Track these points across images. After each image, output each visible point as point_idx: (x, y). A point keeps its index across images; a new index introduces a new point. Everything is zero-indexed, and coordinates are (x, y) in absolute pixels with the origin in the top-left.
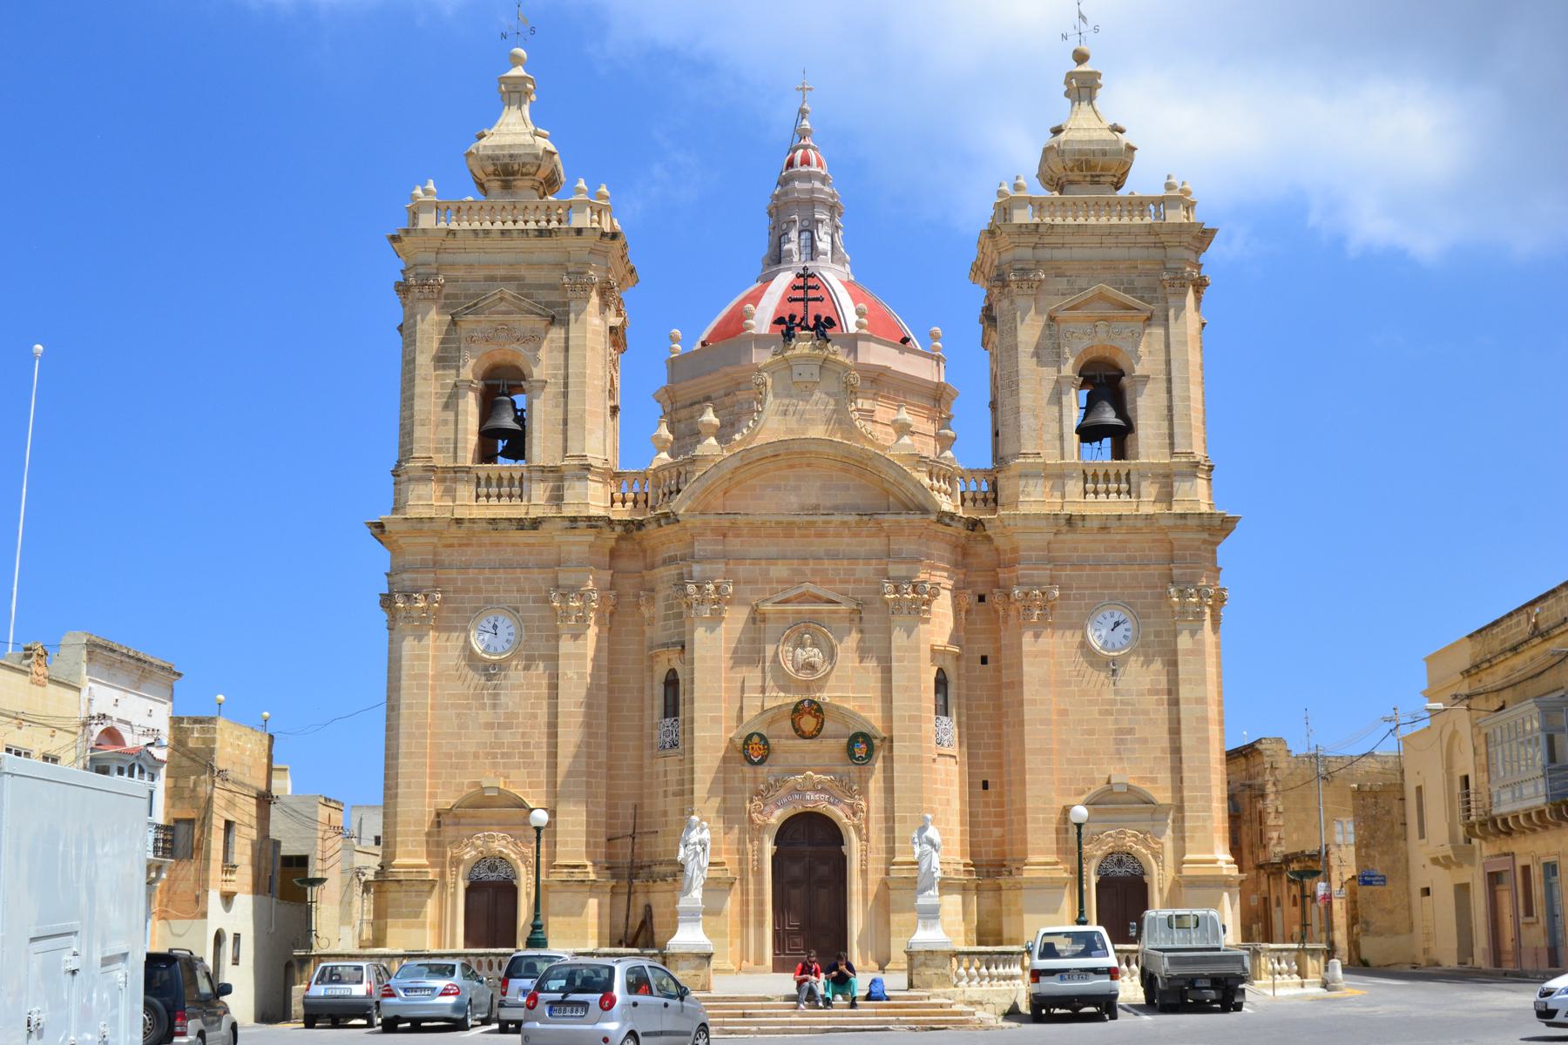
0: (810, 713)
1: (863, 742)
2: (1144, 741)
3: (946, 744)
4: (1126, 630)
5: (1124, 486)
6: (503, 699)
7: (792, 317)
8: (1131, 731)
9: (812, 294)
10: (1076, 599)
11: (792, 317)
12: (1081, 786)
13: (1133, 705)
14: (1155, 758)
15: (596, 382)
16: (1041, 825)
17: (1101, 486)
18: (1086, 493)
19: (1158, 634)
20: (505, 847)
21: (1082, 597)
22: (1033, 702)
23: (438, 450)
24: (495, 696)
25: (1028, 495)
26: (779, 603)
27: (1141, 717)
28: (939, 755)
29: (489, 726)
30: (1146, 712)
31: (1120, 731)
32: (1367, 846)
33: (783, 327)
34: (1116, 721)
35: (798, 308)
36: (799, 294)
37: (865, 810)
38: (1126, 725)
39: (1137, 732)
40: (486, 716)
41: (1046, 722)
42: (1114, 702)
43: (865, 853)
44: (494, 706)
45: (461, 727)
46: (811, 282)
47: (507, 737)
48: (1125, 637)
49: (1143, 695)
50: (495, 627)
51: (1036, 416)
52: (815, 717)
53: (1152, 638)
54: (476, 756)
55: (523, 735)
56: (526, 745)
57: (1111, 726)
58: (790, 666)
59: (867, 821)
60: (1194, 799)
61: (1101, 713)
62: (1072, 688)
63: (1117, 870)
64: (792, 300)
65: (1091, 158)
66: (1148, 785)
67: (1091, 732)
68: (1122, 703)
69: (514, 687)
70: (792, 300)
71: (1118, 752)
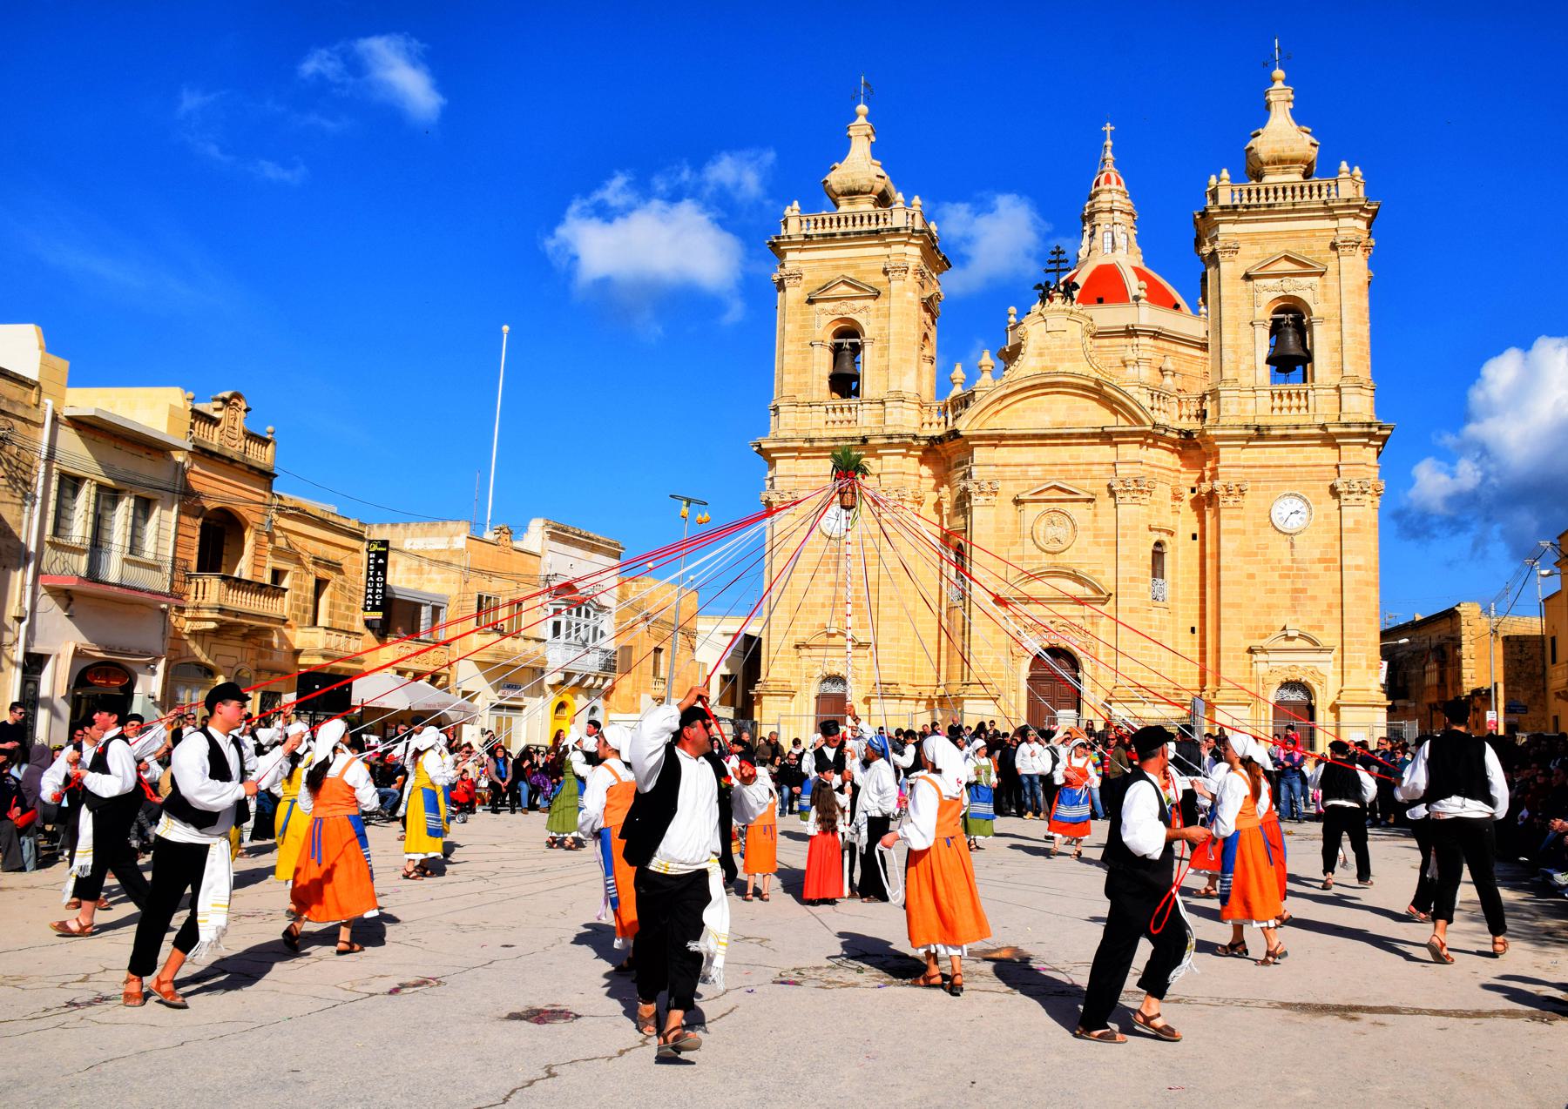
2: (1314, 598)
3: (1161, 599)
5: (1303, 403)
7: (1048, 284)
8: (1304, 591)
10: (1263, 490)
11: (1048, 284)
12: (1264, 631)
13: (1306, 570)
14: (1322, 611)
17: (1286, 402)
19: (1327, 516)
21: (1268, 488)
22: (1228, 568)
23: (800, 391)
25: (1227, 411)
27: (1313, 580)
29: (831, 584)
30: (1316, 577)
31: (1296, 591)
32: (1513, 684)
33: (1041, 291)
34: (1293, 582)
35: (1051, 277)
36: (1053, 266)
38: (1299, 586)
41: (1238, 583)
42: (1291, 568)
46: (1062, 257)
49: (1314, 563)
51: (1235, 352)
53: (1323, 519)
54: (823, 606)
55: (856, 591)
58: (1042, 539)
60: (1351, 643)
61: (1281, 576)
64: (1047, 271)
65: (1282, 154)
66: (1317, 632)
67: (1273, 591)
68: (1298, 569)
70: (1047, 271)
71: (1293, 606)
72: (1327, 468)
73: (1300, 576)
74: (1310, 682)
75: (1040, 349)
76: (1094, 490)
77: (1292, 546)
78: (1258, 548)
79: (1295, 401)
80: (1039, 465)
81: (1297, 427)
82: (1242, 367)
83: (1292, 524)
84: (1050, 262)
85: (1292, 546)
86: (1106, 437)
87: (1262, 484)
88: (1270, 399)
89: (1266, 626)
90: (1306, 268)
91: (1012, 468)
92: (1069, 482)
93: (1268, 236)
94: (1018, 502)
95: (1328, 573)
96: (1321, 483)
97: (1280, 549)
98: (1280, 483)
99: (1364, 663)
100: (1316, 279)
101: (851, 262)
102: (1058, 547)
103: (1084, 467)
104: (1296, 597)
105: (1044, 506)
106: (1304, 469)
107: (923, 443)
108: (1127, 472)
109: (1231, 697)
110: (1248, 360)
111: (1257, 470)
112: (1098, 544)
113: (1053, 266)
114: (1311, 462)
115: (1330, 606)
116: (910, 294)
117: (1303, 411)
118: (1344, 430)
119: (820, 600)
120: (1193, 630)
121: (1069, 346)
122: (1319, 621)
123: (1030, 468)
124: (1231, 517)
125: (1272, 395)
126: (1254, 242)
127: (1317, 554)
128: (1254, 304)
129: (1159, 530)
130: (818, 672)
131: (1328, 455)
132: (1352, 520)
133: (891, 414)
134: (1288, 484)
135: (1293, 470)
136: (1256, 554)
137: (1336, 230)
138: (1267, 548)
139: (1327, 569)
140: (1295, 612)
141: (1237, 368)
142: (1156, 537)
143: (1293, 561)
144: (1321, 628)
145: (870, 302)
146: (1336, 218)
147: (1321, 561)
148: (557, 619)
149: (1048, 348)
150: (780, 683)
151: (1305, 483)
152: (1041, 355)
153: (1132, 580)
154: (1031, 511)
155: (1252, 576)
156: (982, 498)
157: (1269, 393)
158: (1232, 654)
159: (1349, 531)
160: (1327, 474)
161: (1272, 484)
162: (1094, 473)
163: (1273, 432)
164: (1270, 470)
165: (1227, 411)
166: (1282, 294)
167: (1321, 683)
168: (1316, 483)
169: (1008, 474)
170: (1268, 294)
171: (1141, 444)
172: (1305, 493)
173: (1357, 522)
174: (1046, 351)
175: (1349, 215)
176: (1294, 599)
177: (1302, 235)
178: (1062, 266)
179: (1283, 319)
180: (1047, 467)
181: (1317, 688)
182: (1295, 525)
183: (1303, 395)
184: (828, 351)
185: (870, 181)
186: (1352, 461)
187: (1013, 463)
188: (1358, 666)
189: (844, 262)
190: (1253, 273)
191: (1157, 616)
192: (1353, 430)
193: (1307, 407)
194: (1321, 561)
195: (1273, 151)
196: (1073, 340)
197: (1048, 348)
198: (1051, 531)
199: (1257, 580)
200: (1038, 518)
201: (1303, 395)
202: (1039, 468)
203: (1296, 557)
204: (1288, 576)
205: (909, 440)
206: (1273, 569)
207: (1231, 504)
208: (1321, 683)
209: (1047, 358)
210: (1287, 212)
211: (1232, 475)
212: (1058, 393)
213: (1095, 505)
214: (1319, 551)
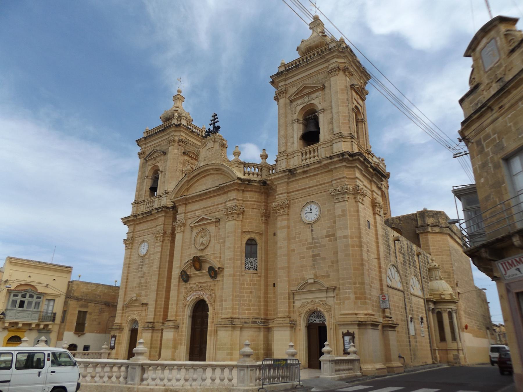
0: (197, 261)
1: (212, 270)
2: (324, 259)
4: (317, 211)
6: (143, 269)
8: (318, 255)
9: (216, 120)
11: (209, 129)
14: (328, 266)
15: (174, 168)
16: (283, 300)
18: (302, 160)
19: (329, 211)
20: (136, 317)
22: (281, 248)
24: (142, 268)
26: (196, 223)
28: (245, 273)
29: (139, 277)
30: (324, 246)
31: (314, 256)
37: (214, 297)
38: (316, 252)
39: (321, 255)
40: (139, 274)
42: (312, 243)
43: (215, 314)
44: (141, 271)
45: (134, 278)
47: (143, 280)
48: (316, 214)
49: (323, 238)
50: (144, 246)
51: (286, 138)
52: (199, 262)
53: (326, 213)
54: (136, 287)
55: (146, 279)
56: (146, 282)
57: (311, 254)
58: (198, 245)
59: (214, 301)
61: (307, 248)
62: (296, 240)
63: (317, 320)
65: (310, 45)
67: (303, 258)
68: (315, 243)
69: (146, 264)
70: (211, 125)
71: (314, 265)
72: (327, 185)
73: (315, 247)
74: (322, 310)
75: (205, 158)
76: (219, 217)
77: (312, 231)
78: (296, 235)
79: (312, 155)
80: (200, 209)
81: (308, 165)
82: (289, 144)
83: (312, 218)
84: (212, 121)
85: (312, 231)
86: (221, 190)
87: (297, 200)
88: (301, 156)
89: (301, 278)
90: (315, 89)
91: (191, 213)
92: (209, 215)
93: (299, 81)
94: (192, 228)
95: (330, 242)
96: (325, 193)
97: (307, 234)
98: (306, 198)
99: (352, 296)
100: (319, 93)
101: (159, 144)
102: (204, 247)
103: (216, 207)
104: (315, 259)
105: (200, 228)
106: (316, 188)
107: (171, 210)
108: (230, 205)
109: (281, 322)
110: (291, 140)
111: (295, 193)
112: (219, 243)
113: (213, 122)
114: (321, 183)
115: (332, 262)
116: (176, 151)
117: (316, 158)
118: (330, 161)
119: (135, 285)
120: (274, 285)
121: (215, 153)
122: (327, 272)
123: (197, 212)
124: (282, 220)
125: (302, 154)
126: (293, 86)
127: (324, 233)
128: (293, 113)
129: (249, 232)
130: (129, 319)
131: (325, 178)
132: (340, 210)
133: (163, 200)
134: (309, 197)
135: (311, 189)
136: (295, 238)
137: (328, 66)
138: (300, 234)
139: (330, 241)
140: (315, 268)
141: (286, 145)
142: (248, 237)
143: (313, 239)
144: (328, 276)
145: (162, 158)
146: (328, 61)
147: (327, 236)
148: (23, 299)
149: (207, 157)
150: (117, 325)
151: (317, 195)
152: (205, 160)
153: (231, 259)
154: (195, 232)
155: (293, 250)
156: (179, 229)
157: (300, 154)
158: (283, 296)
159: (340, 216)
160: (327, 188)
161: (302, 199)
162: (219, 208)
163: (298, 172)
164: (300, 192)
165: (281, 167)
166: (305, 104)
167: (329, 311)
168: (323, 194)
169: (189, 216)
170: (299, 106)
171: (238, 190)
172: (317, 200)
173: (343, 211)
174: (206, 158)
175: (333, 57)
176: (314, 261)
177: (314, 75)
178: (216, 120)
179: (310, 118)
180: (203, 210)
181: (326, 315)
182: (313, 219)
183: (316, 150)
184: (150, 180)
185: (172, 113)
186: (339, 177)
187: (190, 211)
188: (348, 298)
189: (157, 144)
190: (292, 98)
191: (248, 278)
192: (335, 159)
193: (318, 156)
194: (327, 236)
195: (306, 45)
196: (216, 150)
197: (207, 157)
198: (201, 240)
199: (296, 252)
200: (197, 236)
201: (316, 150)
202: (199, 211)
203: (314, 236)
204: (310, 248)
205: (163, 209)
206: (303, 245)
207: (282, 213)
208: (329, 311)
209: (207, 161)
210: (305, 66)
211: (282, 198)
212: (209, 175)
213: (219, 224)
214: (325, 231)
